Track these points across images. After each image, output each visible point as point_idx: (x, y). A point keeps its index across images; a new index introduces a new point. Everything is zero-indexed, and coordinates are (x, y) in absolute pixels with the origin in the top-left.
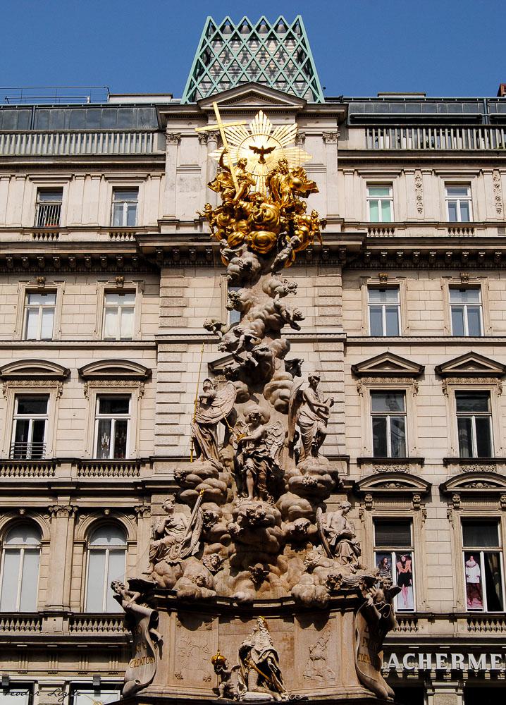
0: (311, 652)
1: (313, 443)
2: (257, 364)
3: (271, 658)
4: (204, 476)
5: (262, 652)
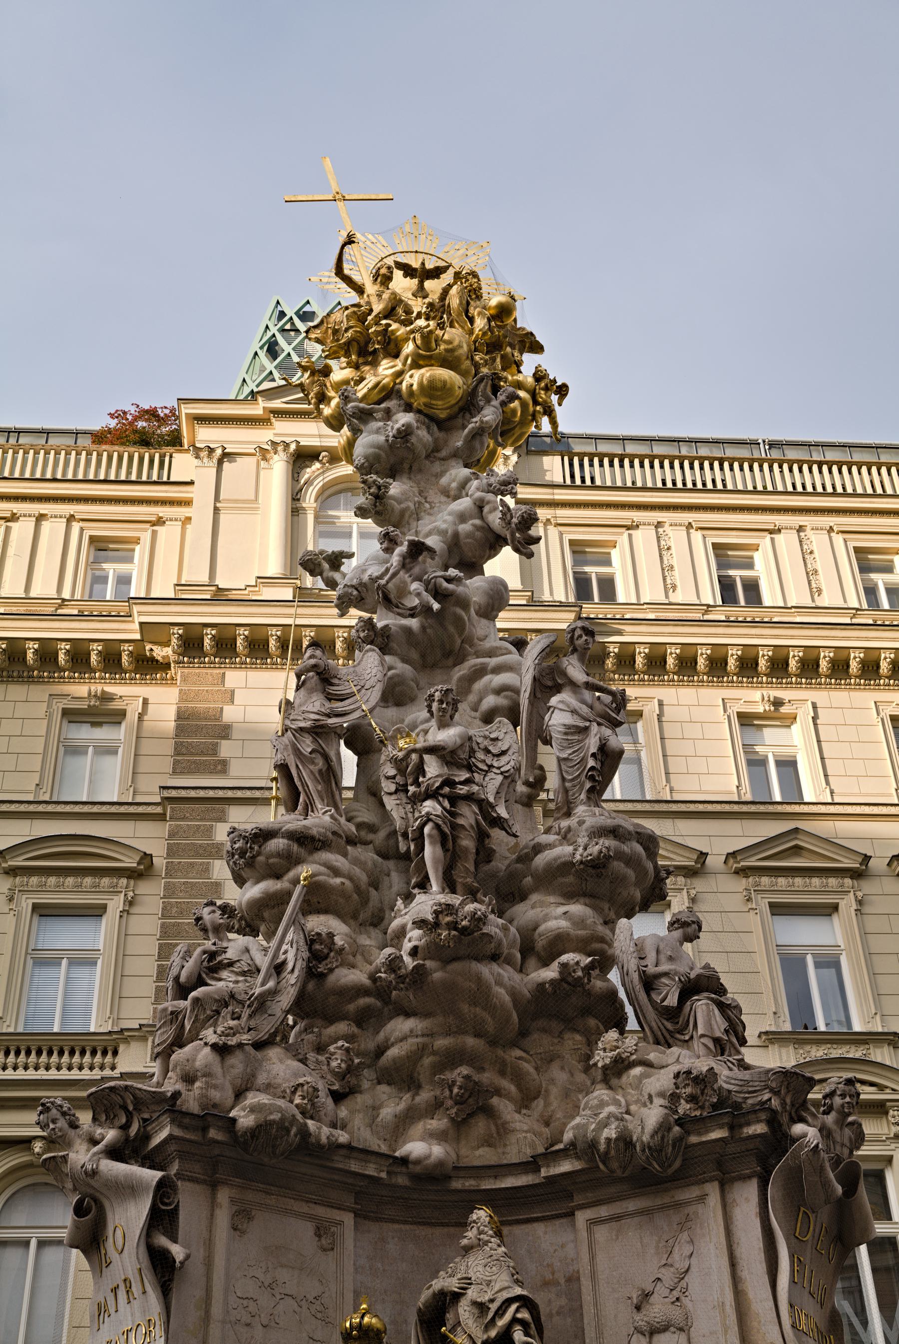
0: (638, 1308)
1: (592, 768)
2: (436, 606)
3: (522, 1322)
5: (494, 1307)
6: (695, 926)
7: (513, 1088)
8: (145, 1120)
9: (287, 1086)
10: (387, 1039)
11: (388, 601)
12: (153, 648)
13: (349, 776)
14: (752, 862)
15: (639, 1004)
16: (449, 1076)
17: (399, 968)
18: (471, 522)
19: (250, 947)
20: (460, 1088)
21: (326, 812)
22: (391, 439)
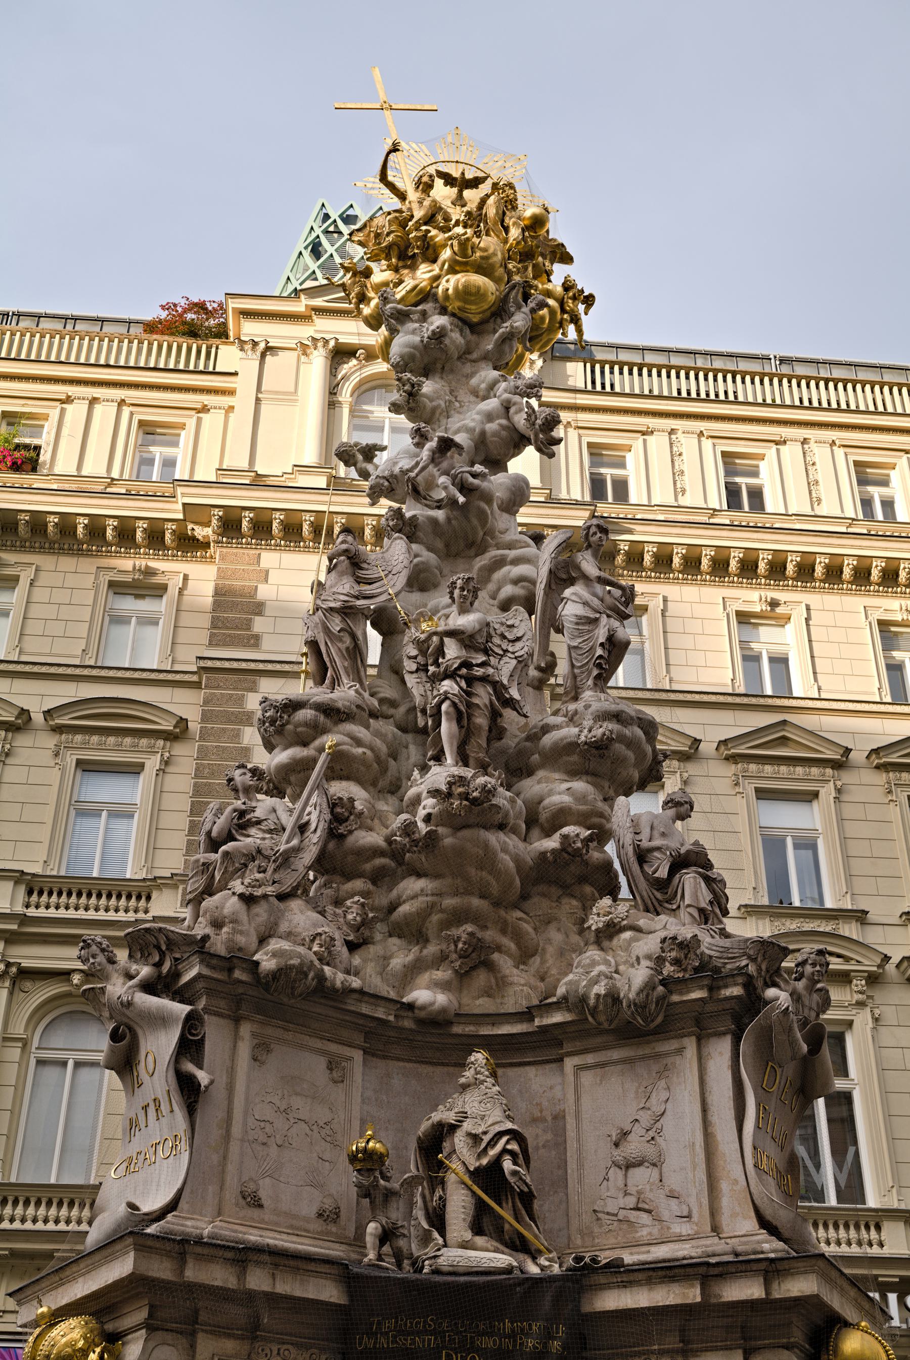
0: (617, 1145)
1: (600, 657)
2: (461, 499)
4: (333, 714)
5: (486, 1138)
6: (687, 806)
7: (513, 946)
8: (176, 959)
9: (307, 934)
10: (399, 897)
11: (417, 493)
13: (374, 655)
14: (742, 750)
15: (632, 874)
16: (455, 932)
17: (413, 833)
18: (497, 422)
19: (277, 808)
20: (465, 943)
21: (351, 687)
22: (425, 340)
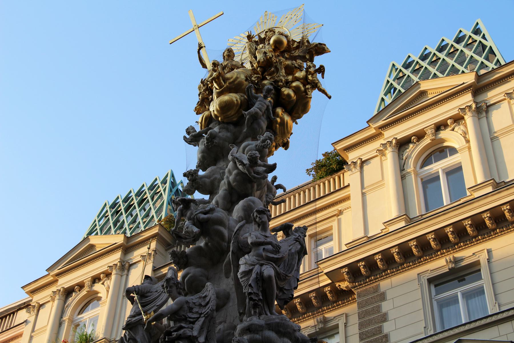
12: (340, 284)
